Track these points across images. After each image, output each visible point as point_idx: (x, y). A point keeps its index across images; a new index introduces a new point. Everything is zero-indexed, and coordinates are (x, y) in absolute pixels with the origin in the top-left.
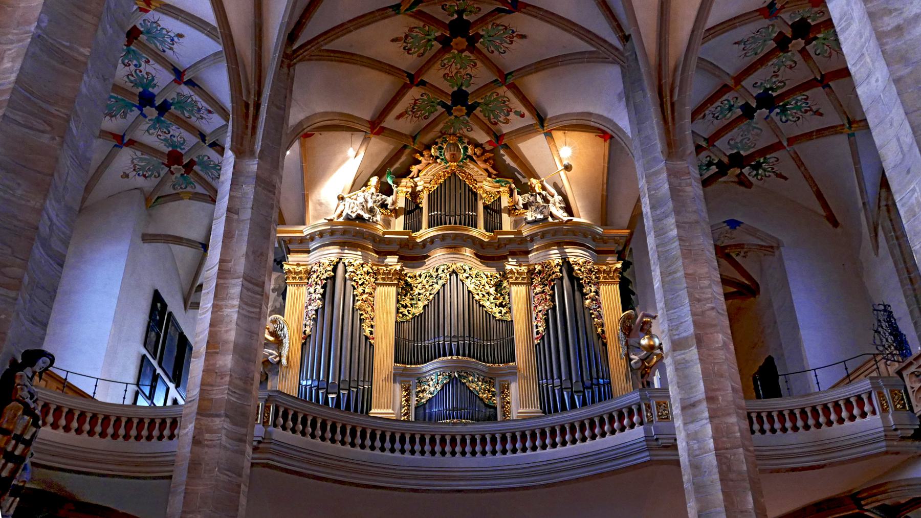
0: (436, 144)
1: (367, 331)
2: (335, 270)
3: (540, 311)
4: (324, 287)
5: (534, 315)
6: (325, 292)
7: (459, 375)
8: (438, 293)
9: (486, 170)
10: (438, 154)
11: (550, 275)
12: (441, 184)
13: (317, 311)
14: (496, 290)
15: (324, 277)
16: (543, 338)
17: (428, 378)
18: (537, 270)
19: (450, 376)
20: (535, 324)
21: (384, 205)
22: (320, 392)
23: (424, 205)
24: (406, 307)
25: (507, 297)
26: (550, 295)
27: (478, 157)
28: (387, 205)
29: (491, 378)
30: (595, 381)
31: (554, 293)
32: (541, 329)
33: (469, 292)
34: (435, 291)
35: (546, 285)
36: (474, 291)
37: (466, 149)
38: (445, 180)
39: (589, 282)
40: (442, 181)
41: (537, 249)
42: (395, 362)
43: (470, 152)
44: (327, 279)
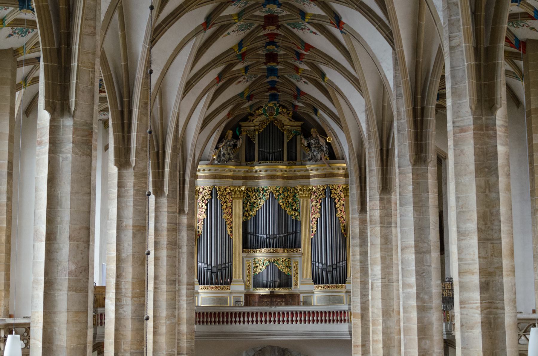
0: (262, 107)
1: (229, 230)
2: (211, 194)
3: (314, 218)
4: (207, 205)
5: (311, 219)
6: (207, 208)
7: (274, 261)
8: (264, 205)
9: (289, 119)
10: (262, 113)
11: (320, 195)
12: (265, 129)
13: (204, 219)
14: (293, 200)
15: (206, 198)
16: (315, 235)
17: (259, 259)
18: (313, 191)
19: (269, 261)
20: (311, 225)
21: (235, 146)
22: (208, 273)
23: (256, 141)
24: (247, 211)
25: (298, 204)
26: (319, 209)
27: (284, 113)
28: (237, 145)
29: (289, 259)
30: (338, 264)
31: (321, 207)
32: (314, 230)
33: (279, 204)
34: (262, 204)
35: (317, 202)
36: (281, 204)
37: (278, 109)
38: (267, 126)
39: (340, 199)
40: (264, 126)
41: (314, 176)
42: (243, 248)
43: (280, 111)
44: (207, 200)
